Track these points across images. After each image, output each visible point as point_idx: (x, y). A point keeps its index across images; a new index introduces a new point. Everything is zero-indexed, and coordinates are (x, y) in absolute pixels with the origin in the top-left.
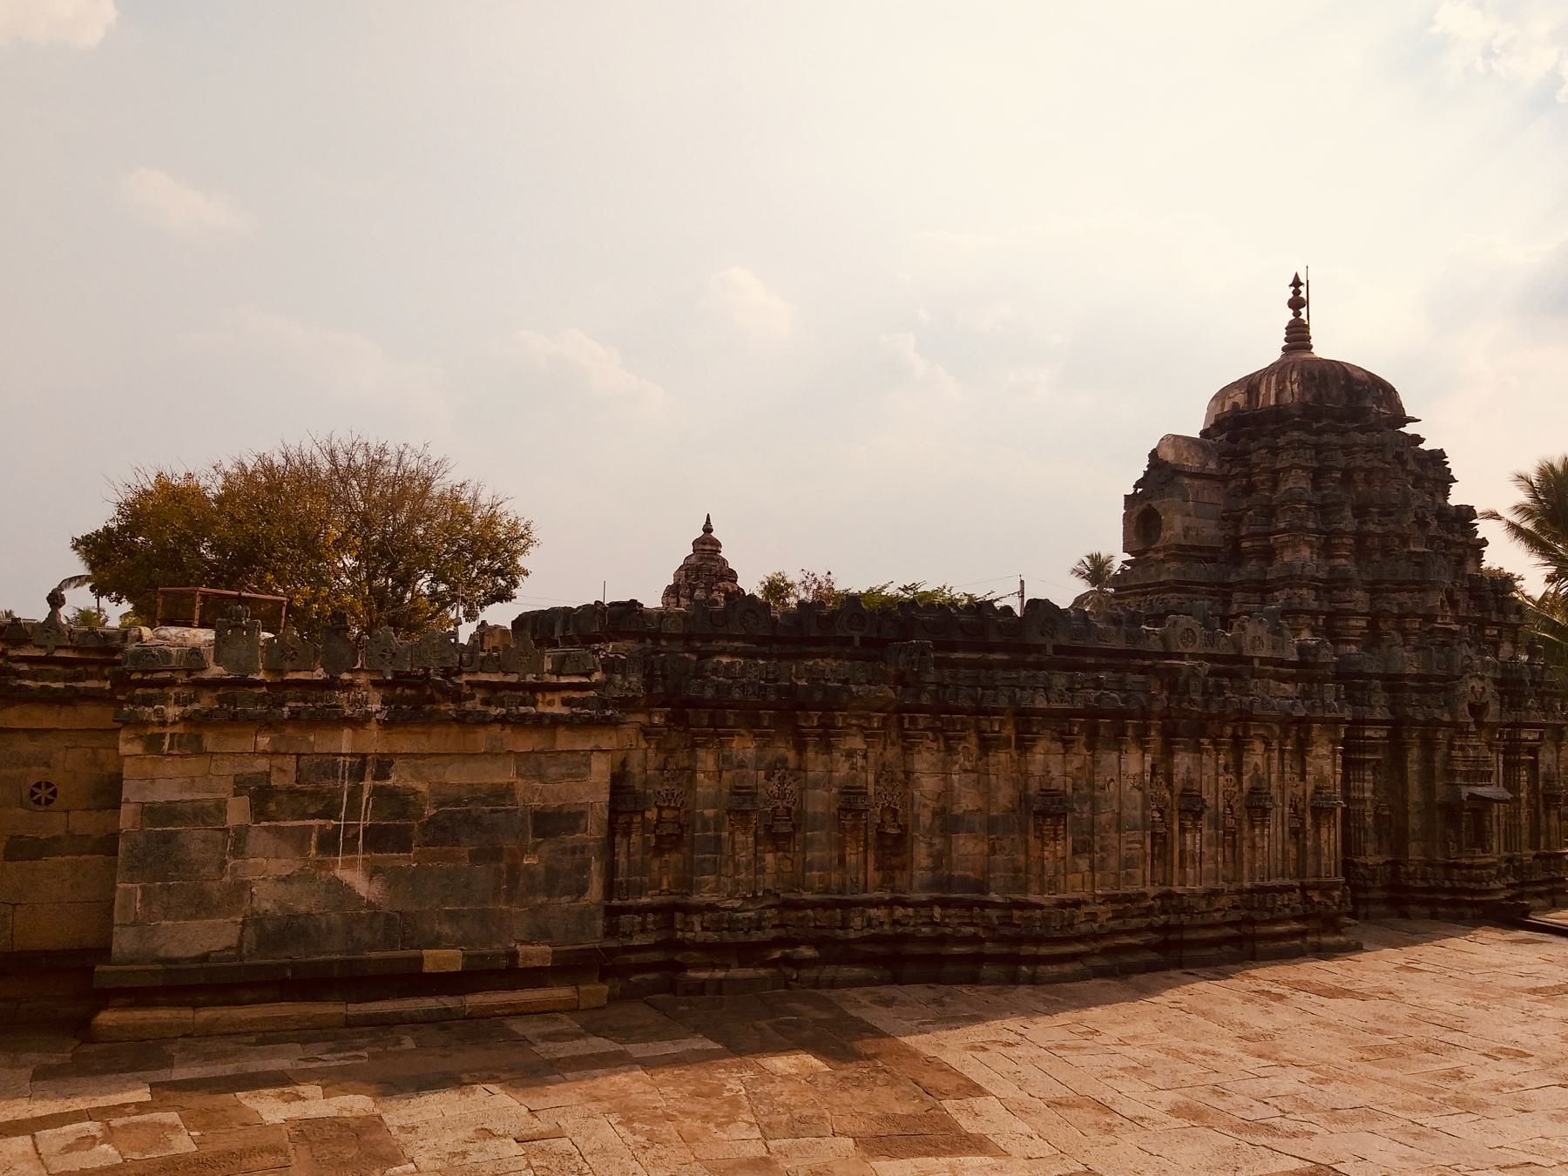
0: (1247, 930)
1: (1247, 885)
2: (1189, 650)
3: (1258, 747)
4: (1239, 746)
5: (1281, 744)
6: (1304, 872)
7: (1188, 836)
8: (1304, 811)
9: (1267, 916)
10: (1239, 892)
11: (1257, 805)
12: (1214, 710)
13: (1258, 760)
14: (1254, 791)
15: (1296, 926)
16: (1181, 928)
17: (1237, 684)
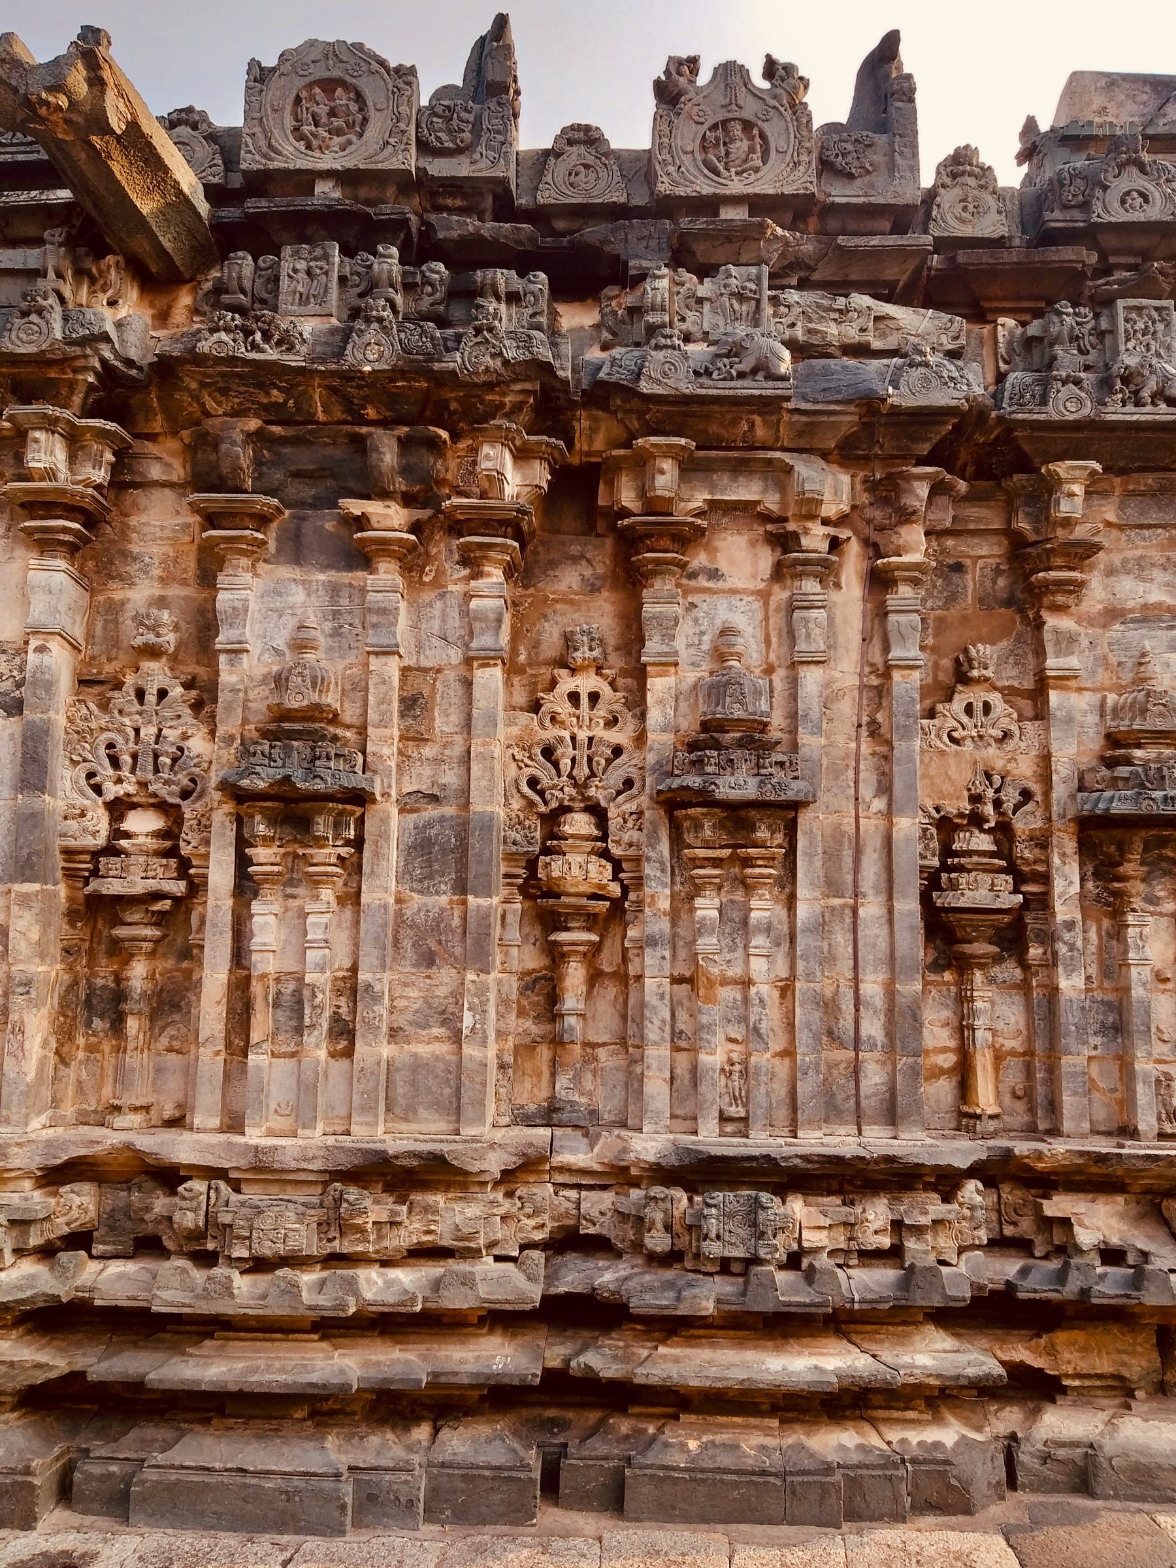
0: (602, 1359)
1: (649, 1145)
2: (327, 162)
3: (740, 558)
4: (641, 553)
5: (874, 549)
6: (1053, 1107)
7: (266, 917)
8: (1042, 842)
9: (707, 1296)
10: (618, 1176)
11: (728, 806)
12: (372, 354)
13: (743, 617)
14: (707, 739)
15: (977, 1359)
16: (137, 1324)
17: (620, 301)
